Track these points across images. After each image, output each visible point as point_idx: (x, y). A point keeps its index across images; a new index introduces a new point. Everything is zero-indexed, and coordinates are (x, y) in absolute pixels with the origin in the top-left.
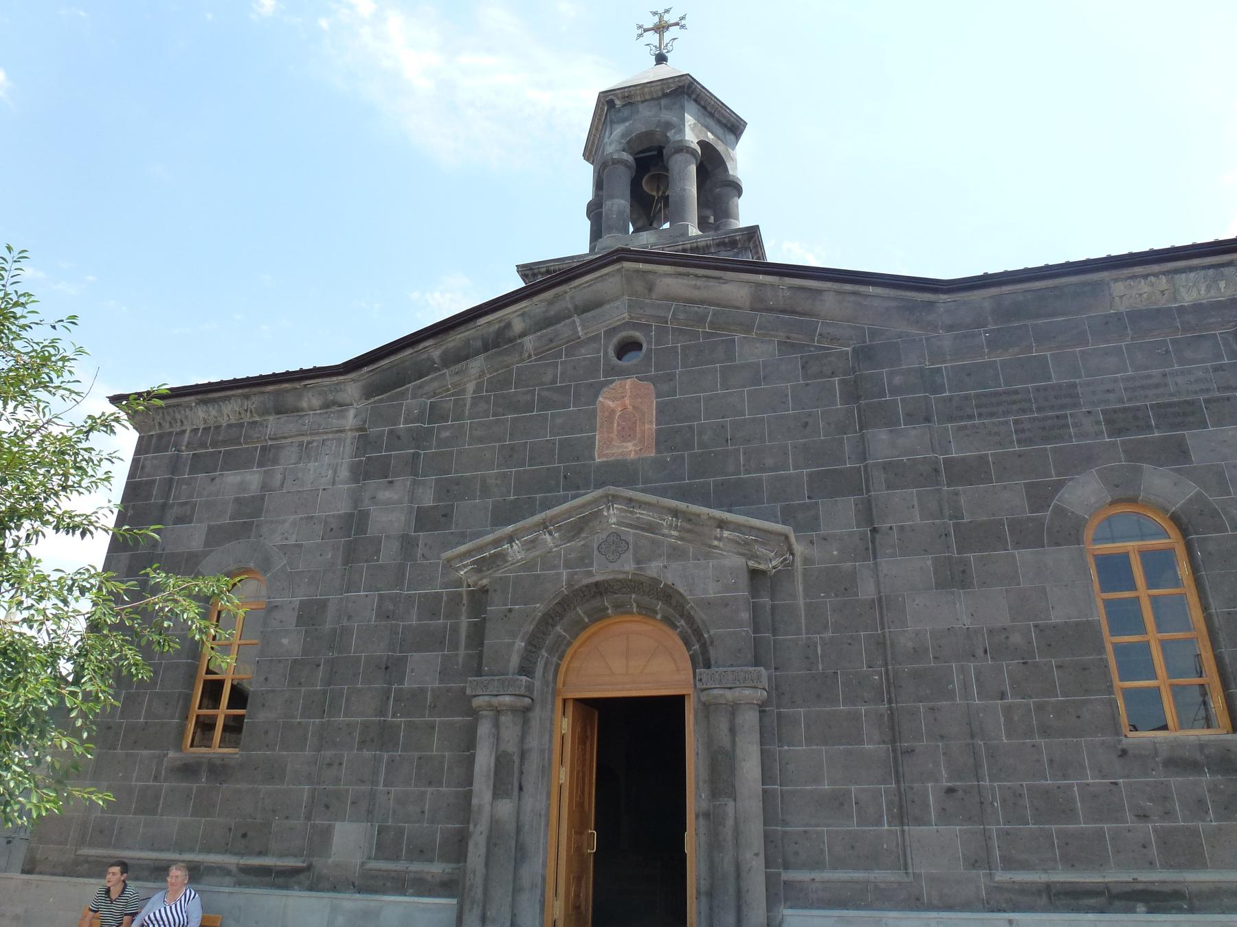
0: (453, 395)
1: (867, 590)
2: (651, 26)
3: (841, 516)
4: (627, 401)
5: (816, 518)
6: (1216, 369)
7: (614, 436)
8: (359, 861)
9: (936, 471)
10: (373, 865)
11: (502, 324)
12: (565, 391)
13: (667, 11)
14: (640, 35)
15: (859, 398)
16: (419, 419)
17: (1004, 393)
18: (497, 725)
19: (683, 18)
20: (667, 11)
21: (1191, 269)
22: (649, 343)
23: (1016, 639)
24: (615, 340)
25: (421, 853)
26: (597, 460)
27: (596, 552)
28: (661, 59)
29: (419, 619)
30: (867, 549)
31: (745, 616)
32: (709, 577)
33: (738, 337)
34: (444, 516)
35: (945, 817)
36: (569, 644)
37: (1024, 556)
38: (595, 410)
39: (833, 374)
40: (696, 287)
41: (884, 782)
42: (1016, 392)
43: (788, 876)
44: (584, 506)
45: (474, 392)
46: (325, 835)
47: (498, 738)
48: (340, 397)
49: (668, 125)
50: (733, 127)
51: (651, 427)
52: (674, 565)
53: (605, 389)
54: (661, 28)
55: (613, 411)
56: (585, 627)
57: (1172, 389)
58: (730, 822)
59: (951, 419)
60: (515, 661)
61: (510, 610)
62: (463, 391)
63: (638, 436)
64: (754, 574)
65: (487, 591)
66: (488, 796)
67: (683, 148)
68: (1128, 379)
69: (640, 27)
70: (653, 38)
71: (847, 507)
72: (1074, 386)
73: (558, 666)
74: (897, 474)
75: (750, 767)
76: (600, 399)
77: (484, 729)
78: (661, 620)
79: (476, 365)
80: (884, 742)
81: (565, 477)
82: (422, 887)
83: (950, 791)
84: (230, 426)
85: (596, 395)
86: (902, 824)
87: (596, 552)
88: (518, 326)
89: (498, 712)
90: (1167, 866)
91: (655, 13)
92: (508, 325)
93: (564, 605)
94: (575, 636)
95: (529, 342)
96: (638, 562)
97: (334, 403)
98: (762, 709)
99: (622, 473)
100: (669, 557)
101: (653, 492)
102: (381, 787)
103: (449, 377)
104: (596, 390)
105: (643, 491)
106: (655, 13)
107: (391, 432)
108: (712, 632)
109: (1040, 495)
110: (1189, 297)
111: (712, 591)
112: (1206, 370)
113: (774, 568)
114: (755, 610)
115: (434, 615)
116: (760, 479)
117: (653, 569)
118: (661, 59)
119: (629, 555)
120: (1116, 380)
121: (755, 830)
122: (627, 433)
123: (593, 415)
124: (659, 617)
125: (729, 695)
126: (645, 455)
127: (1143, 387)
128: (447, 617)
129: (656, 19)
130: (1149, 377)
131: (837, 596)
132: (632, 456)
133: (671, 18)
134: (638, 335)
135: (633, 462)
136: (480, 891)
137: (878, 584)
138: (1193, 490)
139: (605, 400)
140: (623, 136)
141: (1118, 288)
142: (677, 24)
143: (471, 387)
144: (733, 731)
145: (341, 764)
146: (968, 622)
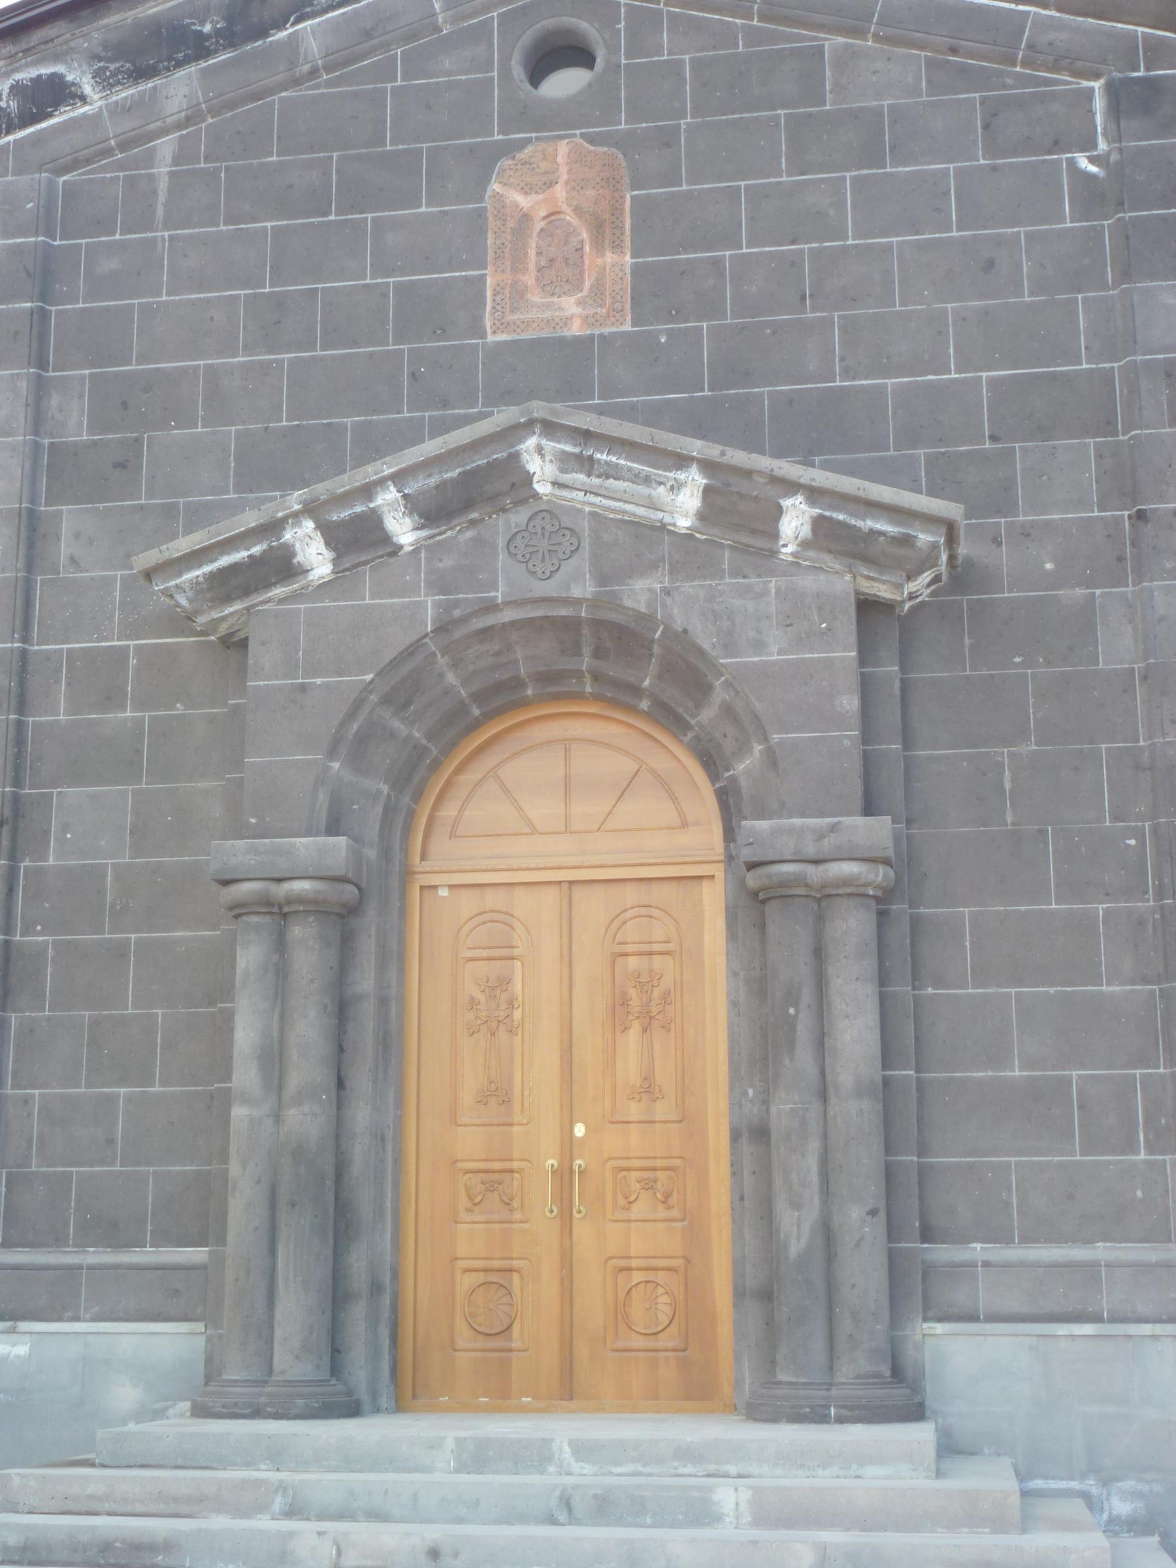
0: (121, 166)
1: (1117, 648)
4: (560, 192)
5: (1008, 486)
7: (529, 279)
16: (45, 222)
24: (527, 38)
26: (491, 338)
27: (502, 557)
29: (68, 712)
30: (1121, 559)
31: (850, 703)
33: (833, 42)
34: (121, 465)
36: (436, 765)
38: (481, 214)
41: (1142, 1062)
44: (475, 446)
45: (176, 161)
52: (692, 588)
53: (505, 163)
55: (525, 218)
56: (475, 725)
61: (303, 688)
62: (149, 159)
64: (867, 607)
65: (243, 644)
73: (411, 815)
76: (495, 186)
78: (648, 716)
80: (1145, 980)
81: (413, 375)
85: (484, 180)
87: (502, 557)
94: (450, 748)
98: (882, 904)
100: (674, 570)
101: (628, 413)
104: (485, 162)
108: (776, 737)
113: (911, 597)
114: (867, 688)
115: (111, 699)
116: (880, 390)
117: (639, 593)
119: (582, 561)
124: (644, 705)
128: (140, 705)
131: (1049, 663)
132: (576, 329)
134: (587, 28)
139: (508, 192)
143: (166, 146)
144: (819, 954)
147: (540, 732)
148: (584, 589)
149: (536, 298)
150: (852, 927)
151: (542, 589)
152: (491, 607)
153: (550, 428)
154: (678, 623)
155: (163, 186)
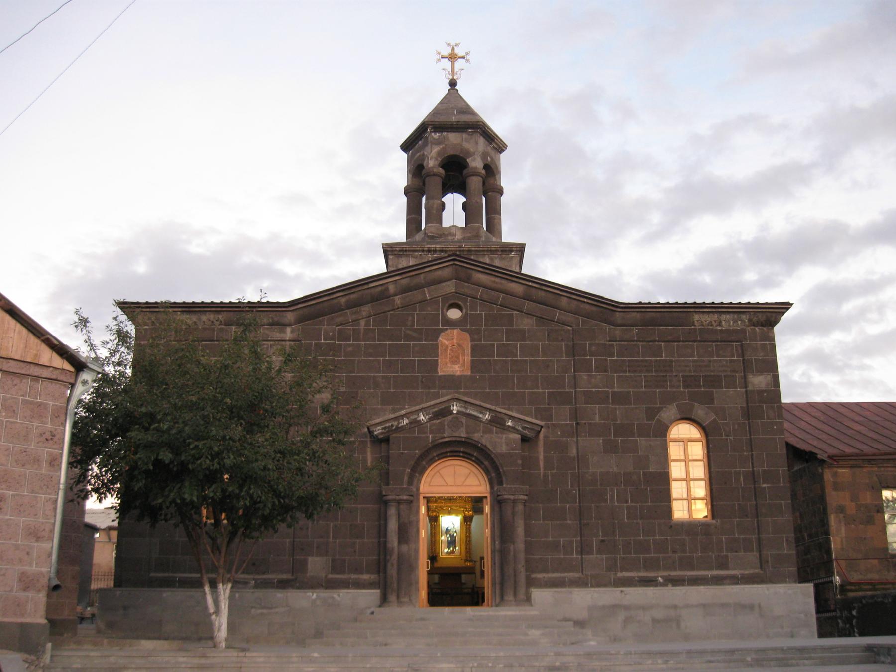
1: (573, 452)
2: (446, 54)
3: (563, 415)
4: (455, 341)
5: (551, 415)
6: (731, 361)
8: (324, 575)
9: (608, 397)
10: (330, 576)
11: (383, 288)
12: (419, 331)
13: (457, 45)
15: (574, 356)
17: (642, 361)
18: (398, 510)
19: (467, 54)
20: (457, 45)
21: (729, 312)
22: (467, 309)
23: (635, 477)
24: (447, 305)
25: (359, 571)
28: (453, 83)
31: (520, 462)
32: (501, 443)
35: (600, 551)
37: (642, 441)
38: (437, 345)
39: (563, 341)
40: (494, 282)
42: (646, 361)
43: (533, 576)
46: (304, 563)
47: (399, 515)
48: (286, 321)
49: (469, 154)
50: (500, 147)
51: (468, 358)
52: (486, 436)
55: (447, 347)
57: (712, 368)
58: (512, 553)
59: (616, 372)
60: (406, 478)
62: (359, 324)
63: (461, 362)
66: (396, 544)
67: (476, 174)
68: (695, 361)
69: (439, 53)
70: (447, 64)
71: (566, 409)
72: (671, 361)
74: (590, 397)
75: (520, 530)
77: (392, 511)
79: (366, 310)
82: (359, 585)
83: (603, 541)
84: (204, 329)
85: (438, 337)
86: (582, 554)
88: (392, 288)
89: (399, 502)
90: (681, 570)
91: (449, 45)
92: (387, 289)
93: (428, 451)
95: (398, 300)
96: (467, 433)
97: (278, 324)
99: (452, 382)
102: (331, 539)
103: (350, 315)
105: (465, 394)
106: (449, 45)
107: (316, 345)
109: (652, 413)
110: (725, 325)
111: (504, 449)
112: (726, 361)
116: (524, 393)
117: (476, 436)
118: (453, 83)
120: (690, 361)
121: (522, 556)
122: (455, 360)
123: (435, 348)
125: (512, 497)
126: (465, 374)
127: (700, 366)
129: (450, 51)
130: (704, 361)
132: (458, 373)
133: (459, 51)
135: (460, 377)
136: (395, 585)
137: (578, 449)
138: (713, 417)
139: (443, 340)
140: (439, 154)
141: (696, 317)
142: (463, 58)
143: (363, 322)
145: (307, 528)
146: (615, 470)
147: (448, 463)
148: (464, 435)
149: (449, 365)
150: (520, 507)
151: (455, 434)
152: (444, 437)
153: (458, 400)
154: (484, 443)
155: (362, 331)
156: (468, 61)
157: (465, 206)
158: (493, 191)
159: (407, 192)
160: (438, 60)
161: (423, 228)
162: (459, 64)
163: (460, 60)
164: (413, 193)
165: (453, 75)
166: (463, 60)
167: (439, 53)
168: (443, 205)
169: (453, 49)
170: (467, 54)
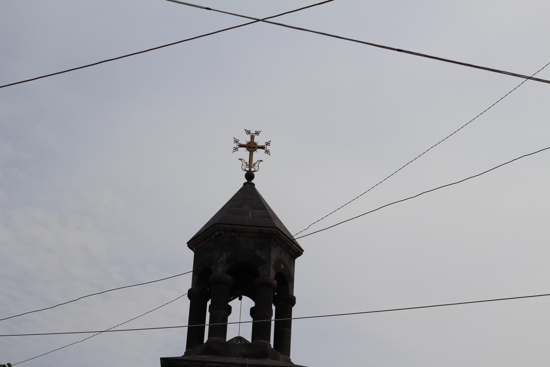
2: (244, 143)
13: (257, 133)
14: (236, 149)
19: (268, 144)
20: (257, 133)
28: (250, 176)
54: (252, 147)
70: (244, 153)
91: (248, 132)
106: (248, 132)
118: (250, 176)
129: (249, 140)
133: (259, 140)
142: (262, 148)
156: (267, 152)
157: (253, 312)
158: (286, 302)
159: (191, 294)
160: (236, 149)
161: (205, 341)
162: (258, 154)
163: (259, 150)
164: (196, 297)
165: (250, 167)
166: (263, 151)
167: (236, 141)
168: (230, 308)
169: (252, 138)
170: (268, 144)
